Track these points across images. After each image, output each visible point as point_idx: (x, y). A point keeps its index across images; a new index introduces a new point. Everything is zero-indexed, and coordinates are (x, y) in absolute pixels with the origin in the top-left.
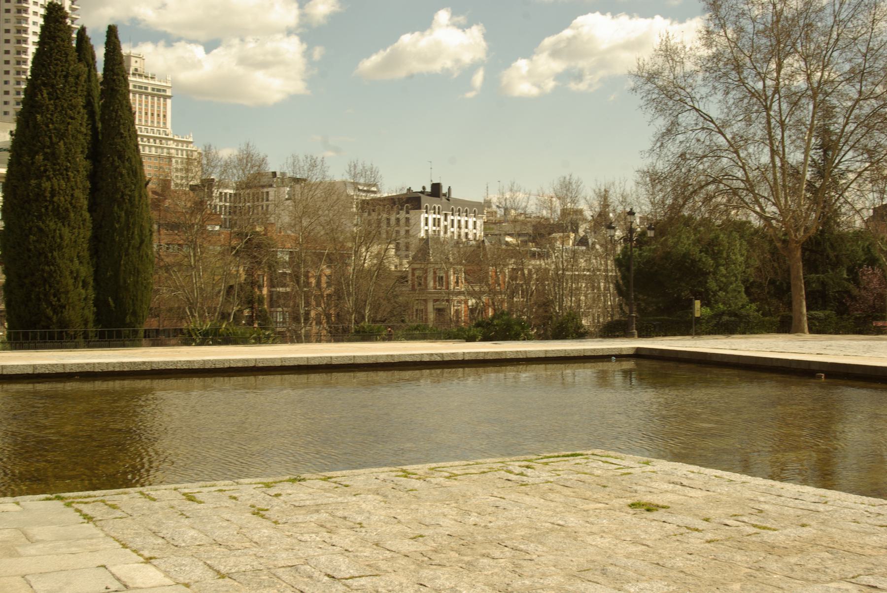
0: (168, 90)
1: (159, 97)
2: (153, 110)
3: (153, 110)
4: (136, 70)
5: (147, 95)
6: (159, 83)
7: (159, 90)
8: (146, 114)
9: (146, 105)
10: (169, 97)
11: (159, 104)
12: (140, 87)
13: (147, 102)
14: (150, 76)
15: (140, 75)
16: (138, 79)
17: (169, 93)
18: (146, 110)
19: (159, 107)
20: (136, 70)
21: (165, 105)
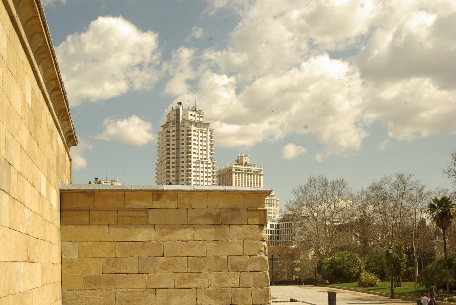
0: (261, 171)
1: (257, 175)
2: (254, 181)
3: (254, 181)
4: (246, 163)
5: (251, 174)
6: (257, 168)
7: (257, 172)
8: (251, 183)
9: (251, 179)
10: (262, 175)
11: (257, 178)
12: (248, 171)
13: (251, 178)
14: (252, 165)
15: (248, 165)
16: (247, 167)
17: (262, 173)
18: (251, 181)
19: (257, 180)
20: (246, 163)
21: (260, 178)
